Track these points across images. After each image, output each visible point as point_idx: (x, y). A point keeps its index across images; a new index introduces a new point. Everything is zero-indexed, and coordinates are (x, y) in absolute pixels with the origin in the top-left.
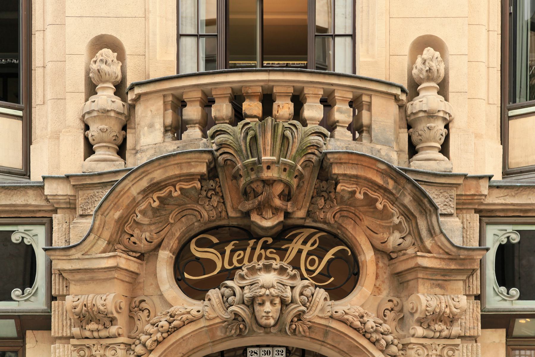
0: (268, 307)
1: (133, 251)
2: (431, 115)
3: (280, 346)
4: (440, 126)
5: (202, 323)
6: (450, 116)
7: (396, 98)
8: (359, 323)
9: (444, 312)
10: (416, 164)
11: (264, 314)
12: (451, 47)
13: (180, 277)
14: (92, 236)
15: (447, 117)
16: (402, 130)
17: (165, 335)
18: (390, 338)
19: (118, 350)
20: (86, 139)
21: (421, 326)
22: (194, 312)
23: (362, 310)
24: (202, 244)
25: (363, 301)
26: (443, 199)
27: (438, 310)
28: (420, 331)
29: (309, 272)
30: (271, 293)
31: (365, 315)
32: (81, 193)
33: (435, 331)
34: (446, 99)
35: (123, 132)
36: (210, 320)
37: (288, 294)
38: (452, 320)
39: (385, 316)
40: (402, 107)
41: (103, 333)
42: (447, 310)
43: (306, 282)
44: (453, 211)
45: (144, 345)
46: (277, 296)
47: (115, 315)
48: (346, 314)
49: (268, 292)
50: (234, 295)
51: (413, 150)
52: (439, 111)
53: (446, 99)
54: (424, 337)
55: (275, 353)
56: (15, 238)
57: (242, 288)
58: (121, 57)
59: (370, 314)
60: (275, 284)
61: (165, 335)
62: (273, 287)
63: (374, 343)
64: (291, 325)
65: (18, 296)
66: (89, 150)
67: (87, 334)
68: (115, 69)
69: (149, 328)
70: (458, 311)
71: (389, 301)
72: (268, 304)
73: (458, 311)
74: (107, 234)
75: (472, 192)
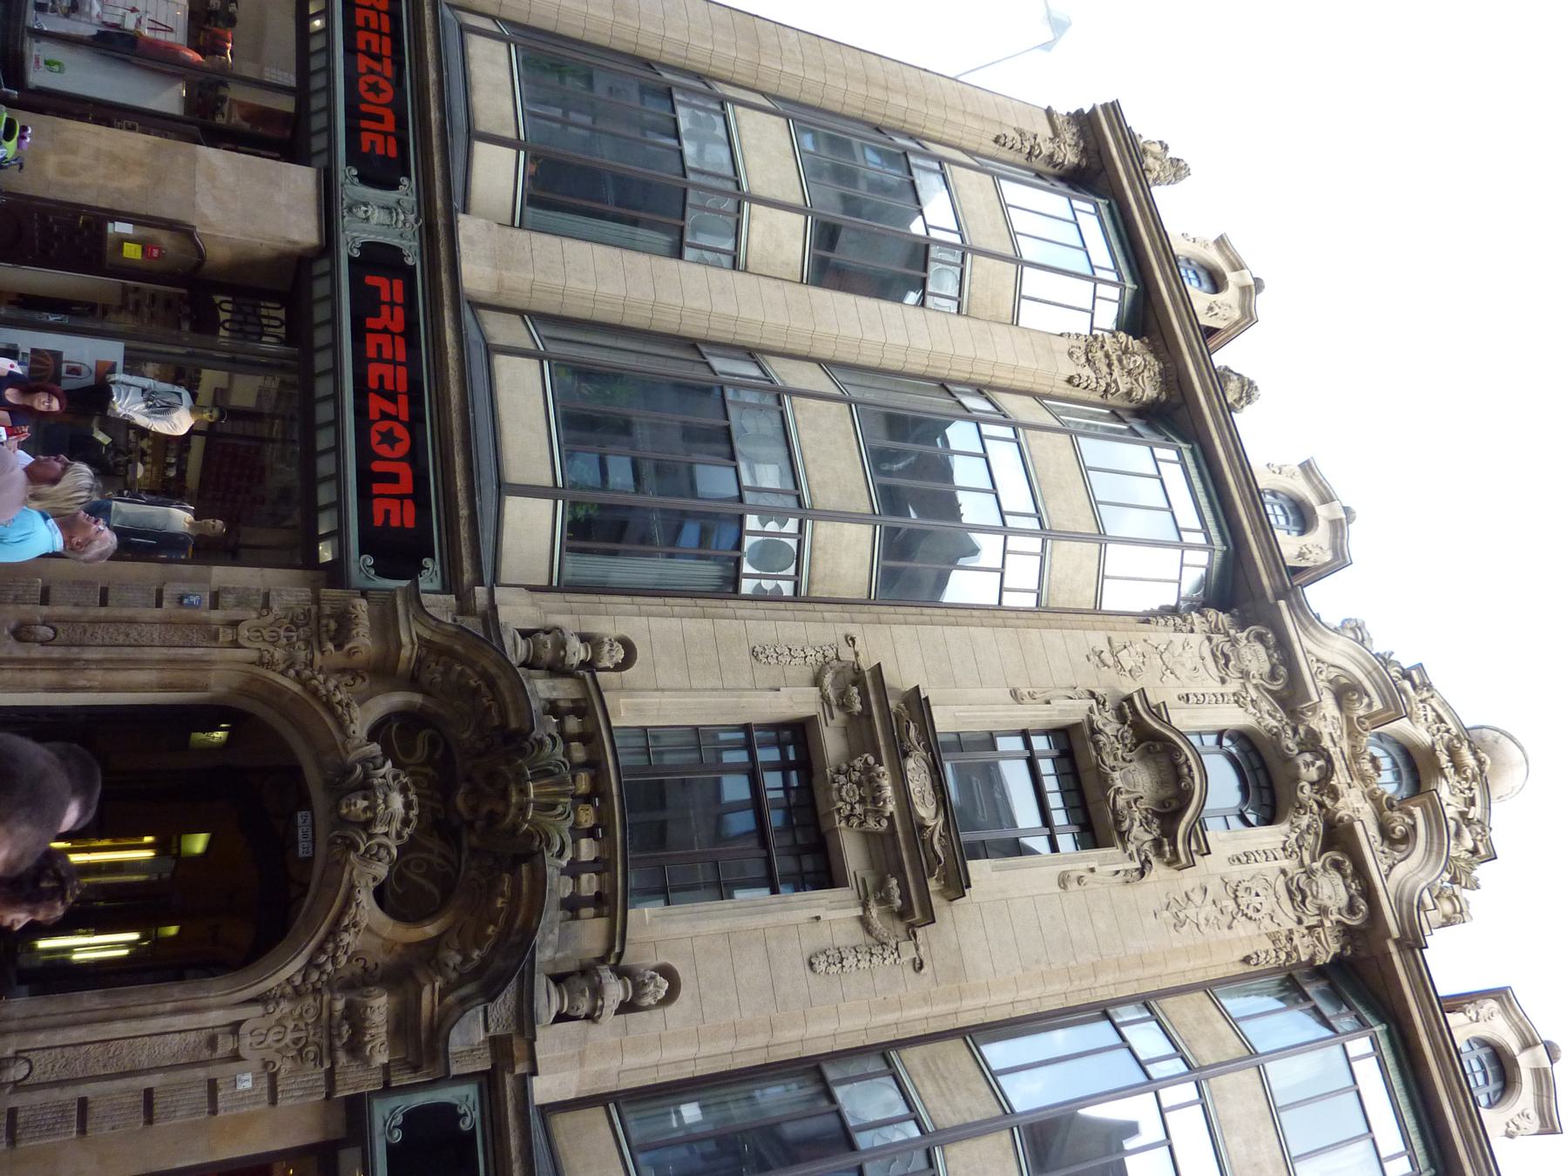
0: (362, 804)
1: (419, 668)
2: (597, 992)
3: (314, 849)
4: (584, 1006)
5: (338, 737)
6: (599, 1016)
7: (611, 948)
8: (346, 922)
9: (365, 1035)
10: (541, 982)
11: (353, 801)
12: (672, 1009)
13: (393, 718)
14: (434, 623)
15: (597, 1014)
16: (578, 964)
17: (324, 699)
18: (329, 967)
19: (303, 653)
20: (536, 631)
21: (346, 1007)
22: (352, 727)
23: (363, 925)
24: (433, 744)
25: (375, 927)
26: (505, 1017)
27: (367, 1024)
28: (339, 1005)
29: (407, 865)
30: (379, 805)
31: (356, 930)
32: (479, 620)
33: (340, 1026)
34: (617, 1012)
35: (545, 667)
36: (344, 745)
37: (380, 829)
38: (355, 1048)
39: (357, 960)
40: (603, 960)
41: (324, 636)
42: (367, 1038)
43: (395, 852)
44: (492, 1030)
45: (311, 679)
46: (375, 814)
47: (347, 647)
48: (358, 905)
49: (380, 801)
50: (376, 768)
51: (558, 979)
52: (603, 999)
53: (617, 1012)
54: (331, 1015)
55: (306, 844)
56: (427, 562)
57: (384, 777)
58: (619, 667)
59: (359, 937)
60: (390, 810)
61: (324, 699)
62: (386, 808)
63: (321, 949)
64: (341, 837)
65: (364, 560)
66: (525, 634)
67: (324, 622)
68: (606, 662)
69: (331, 684)
70: (368, 1054)
71: (376, 964)
72: (365, 803)
73: (368, 1054)
74: (437, 638)
75: (516, 1053)
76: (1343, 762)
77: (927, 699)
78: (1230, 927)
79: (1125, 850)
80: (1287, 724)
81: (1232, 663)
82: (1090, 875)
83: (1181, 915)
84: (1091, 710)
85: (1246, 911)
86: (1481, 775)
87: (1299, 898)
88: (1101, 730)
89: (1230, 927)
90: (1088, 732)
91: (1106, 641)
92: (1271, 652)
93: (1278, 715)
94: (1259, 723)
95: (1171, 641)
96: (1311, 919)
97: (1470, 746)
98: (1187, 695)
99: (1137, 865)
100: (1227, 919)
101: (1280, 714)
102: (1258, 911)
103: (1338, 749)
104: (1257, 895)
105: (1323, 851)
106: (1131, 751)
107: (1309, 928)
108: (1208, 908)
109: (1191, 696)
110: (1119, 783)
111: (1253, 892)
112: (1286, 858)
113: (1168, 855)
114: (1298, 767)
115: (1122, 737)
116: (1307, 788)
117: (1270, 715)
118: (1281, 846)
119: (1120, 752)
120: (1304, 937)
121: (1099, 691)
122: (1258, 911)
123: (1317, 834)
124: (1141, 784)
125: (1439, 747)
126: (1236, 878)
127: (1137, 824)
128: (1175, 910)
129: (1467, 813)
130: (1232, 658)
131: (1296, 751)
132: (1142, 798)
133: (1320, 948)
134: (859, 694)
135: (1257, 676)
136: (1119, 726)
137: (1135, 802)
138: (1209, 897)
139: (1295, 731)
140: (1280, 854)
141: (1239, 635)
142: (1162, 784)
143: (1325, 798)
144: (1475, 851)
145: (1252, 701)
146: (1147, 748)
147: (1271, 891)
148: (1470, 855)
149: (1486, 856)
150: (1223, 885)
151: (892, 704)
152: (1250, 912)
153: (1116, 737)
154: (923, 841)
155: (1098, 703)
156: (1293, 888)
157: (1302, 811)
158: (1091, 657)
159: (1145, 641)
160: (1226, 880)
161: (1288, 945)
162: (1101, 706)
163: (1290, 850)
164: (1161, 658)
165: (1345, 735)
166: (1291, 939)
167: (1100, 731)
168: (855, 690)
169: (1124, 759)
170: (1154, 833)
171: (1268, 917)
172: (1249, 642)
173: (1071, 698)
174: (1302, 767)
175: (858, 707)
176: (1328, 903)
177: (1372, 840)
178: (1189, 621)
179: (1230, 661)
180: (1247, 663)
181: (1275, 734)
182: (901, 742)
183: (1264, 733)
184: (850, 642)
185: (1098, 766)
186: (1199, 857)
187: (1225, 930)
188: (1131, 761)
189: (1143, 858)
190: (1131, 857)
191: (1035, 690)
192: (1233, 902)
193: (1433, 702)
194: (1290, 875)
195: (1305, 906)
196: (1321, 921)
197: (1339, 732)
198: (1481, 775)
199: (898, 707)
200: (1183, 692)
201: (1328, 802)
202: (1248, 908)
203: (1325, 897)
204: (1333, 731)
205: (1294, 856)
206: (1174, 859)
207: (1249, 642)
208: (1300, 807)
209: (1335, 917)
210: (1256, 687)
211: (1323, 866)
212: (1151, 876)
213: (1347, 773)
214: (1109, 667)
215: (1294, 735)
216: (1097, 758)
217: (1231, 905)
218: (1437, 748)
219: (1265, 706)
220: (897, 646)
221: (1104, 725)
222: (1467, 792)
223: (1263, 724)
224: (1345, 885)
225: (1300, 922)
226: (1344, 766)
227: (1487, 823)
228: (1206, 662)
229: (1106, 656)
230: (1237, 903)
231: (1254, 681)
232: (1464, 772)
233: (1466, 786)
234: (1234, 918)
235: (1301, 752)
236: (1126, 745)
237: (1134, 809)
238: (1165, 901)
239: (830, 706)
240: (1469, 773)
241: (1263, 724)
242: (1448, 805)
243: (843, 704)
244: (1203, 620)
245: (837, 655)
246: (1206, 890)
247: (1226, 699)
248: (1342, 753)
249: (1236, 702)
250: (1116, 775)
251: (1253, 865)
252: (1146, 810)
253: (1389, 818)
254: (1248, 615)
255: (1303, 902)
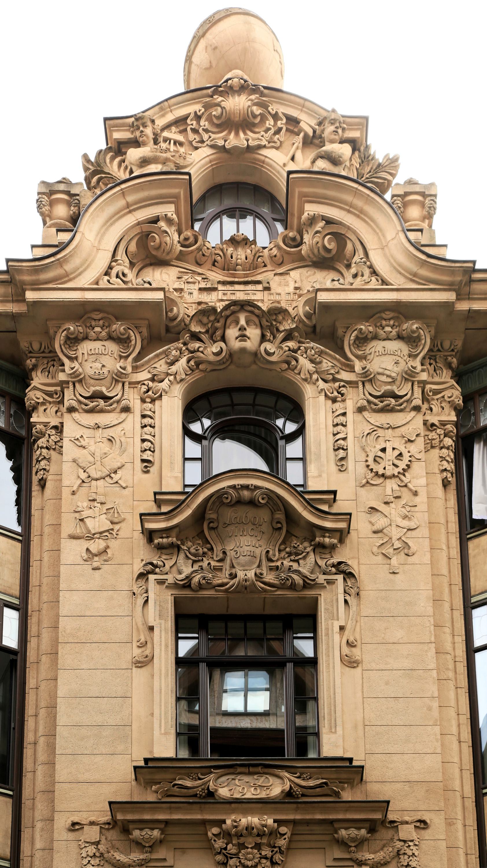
76: (237, 287)
77: (146, 760)
78: (415, 494)
79: (322, 587)
80: (185, 344)
81: (104, 390)
82: (347, 632)
83: (397, 545)
84: (161, 582)
85: (400, 470)
86: (262, 94)
87: (393, 401)
88: (187, 577)
89: (415, 494)
90: (187, 593)
91: (75, 541)
92: (92, 334)
93: (174, 352)
94: (182, 380)
95: (74, 461)
96: (416, 395)
97: (221, 94)
98: (143, 461)
99: (340, 578)
100: (406, 496)
101: (173, 351)
102: (401, 455)
103: (220, 287)
104: (384, 450)
105: (340, 350)
106: (211, 549)
107: (425, 399)
108: (393, 511)
109: (145, 457)
110: (251, 574)
111: (380, 454)
112: (344, 401)
113: (335, 541)
114: (243, 350)
115: (195, 555)
116: (270, 347)
117: (172, 363)
118: (330, 402)
119: (213, 563)
120: (431, 409)
121: (138, 568)
122: (401, 455)
123: (321, 353)
124: (253, 549)
125: (219, 139)
126: (361, 469)
127: (295, 566)
128: (391, 550)
129: (306, 135)
130: (98, 388)
131: (223, 345)
132: (268, 552)
133: (447, 393)
134: (141, 829)
135: (122, 363)
136: (182, 556)
137: (270, 560)
138: (382, 507)
139: (195, 337)
140: (339, 407)
141: (67, 368)
142: (255, 525)
143: (282, 328)
144: (354, 144)
145: (153, 380)
146: (211, 529)
147: (380, 432)
148: (357, 153)
149: (362, 133)
150: (368, 488)
151: (151, 797)
152: (402, 465)
153: (194, 562)
154: (303, 795)
155: (153, 572)
156: (381, 405)
157: (294, 363)
158: (95, 565)
159: (74, 493)
160: (364, 481)
161: (438, 431)
162: (157, 570)
163: (336, 394)
164: (97, 480)
165: (199, 270)
166: (433, 425)
167: (189, 578)
168: (136, 833)
169: (221, 560)
170: (308, 549)
171: (409, 444)
172: (76, 358)
173: (146, 601)
174: (243, 344)
175: (156, 833)
176: (402, 366)
177: (337, 285)
178: (42, 427)
179: (102, 392)
180: (105, 370)
181: (198, 364)
182: (195, 795)
183: (190, 379)
184: (77, 827)
185: (226, 591)
186: (336, 505)
187: (417, 500)
188: (224, 553)
189: (334, 570)
190: (330, 582)
191: (135, 639)
192: (388, 481)
193: (160, 122)
194: (365, 403)
195: (401, 397)
196: (419, 382)
197: (199, 278)
198: (262, 94)
199: (156, 792)
200: (139, 465)
201: (287, 325)
202: (397, 466)
203: (396, 369)
204: (197, 286)
205: (343, 390)
206: (338, 535)
207: (76, 358)
208: (288, 363)
209: (417, 363)
210: (136, 369)
211: (360, 358)
212: (354, 566)
213: (250, 287)
214: (108, 547)
215: (201, 340)
216: (217, 591)
217: (391, 485)
218: (221, 143)
219: (161, 366)
220: (81, 780)
221: (180, 573)
222: (279, 123)
223: (184, 376)
224: (384, 340)
225: (417, 409)
226: (241, 287)
227: (325, 114)
228: (102, 423)
229: (96, 546)
230: (390, 477)
231: (129, 369)
232: (255, 116)
233: (272, 122)
234: (406, 486)
235: (223, 339)
236: (204, 553)
237: (279, 563)
238: (380, 558)
239: (151, 860)
240: (257, 111)
241: (184, 376)
242: (293, 159)
243: (150, 847)
244: (41, 409)
245: (93, 843)
246: (372, 508)
247: (149, 413)
248: (224, 283)
249: (153, 401)
250: (241, 575)
251: (350, 443)
252: (280, 551)
253: (312, 250)
254: (36, 346)
255: (396, 397)
